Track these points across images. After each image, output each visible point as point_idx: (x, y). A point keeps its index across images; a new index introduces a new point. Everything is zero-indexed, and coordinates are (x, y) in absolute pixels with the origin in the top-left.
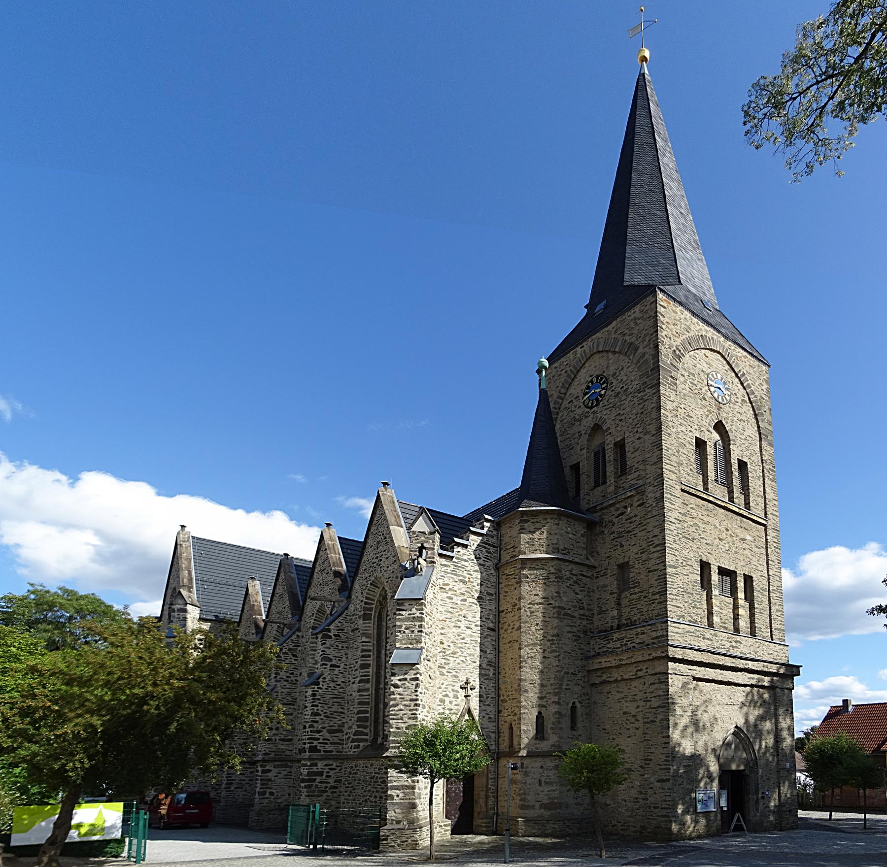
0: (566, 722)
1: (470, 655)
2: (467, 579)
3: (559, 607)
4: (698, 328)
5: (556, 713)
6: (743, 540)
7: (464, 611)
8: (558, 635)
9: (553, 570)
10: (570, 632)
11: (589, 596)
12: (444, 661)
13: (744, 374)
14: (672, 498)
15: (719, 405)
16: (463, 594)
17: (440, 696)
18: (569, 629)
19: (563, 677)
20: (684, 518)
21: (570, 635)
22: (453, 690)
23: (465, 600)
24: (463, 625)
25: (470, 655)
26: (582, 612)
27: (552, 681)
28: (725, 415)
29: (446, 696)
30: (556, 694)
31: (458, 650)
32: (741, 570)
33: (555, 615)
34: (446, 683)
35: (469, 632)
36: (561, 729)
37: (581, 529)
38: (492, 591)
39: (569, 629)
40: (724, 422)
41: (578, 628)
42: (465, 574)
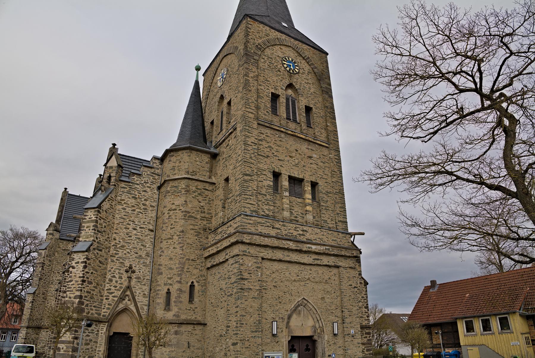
0: (185, 297)
1: (134, 248)
2: (137, 197)
3: (185, 211)
4: (275, 34)
5: (177, 290)
6: (310, 157)
7: (133, 218)
8: (183, 232)
9: (184, 186)
10: (193, 229)
11: (210, 204)
12: (115, 252)
13: (308, 58)
14: (250, 129)
15: (291, 74)
16: (133, 206)
17: (109, 277)
18: (191, 227)
19: (185, 263)
20: (260, 143)
21: (192, 231)
22: (119, 273)
23: (134, 210)
24: (131, 227)
25: (134, 248)
26: (203, 215)
27: (177, 266)
28: (295, 80)
29: (114, 277)
30: (179, 275)
31: (126, 244)
32: (308, 177)
33: (183, 217)
34: (115, 267)
35: (135, 232)
36: (181, 302)
37: (206, 158)
38: (154, 204)
39: (191, 227)
40: (294, 84)
41: (200, 227)
42: (136, 193)
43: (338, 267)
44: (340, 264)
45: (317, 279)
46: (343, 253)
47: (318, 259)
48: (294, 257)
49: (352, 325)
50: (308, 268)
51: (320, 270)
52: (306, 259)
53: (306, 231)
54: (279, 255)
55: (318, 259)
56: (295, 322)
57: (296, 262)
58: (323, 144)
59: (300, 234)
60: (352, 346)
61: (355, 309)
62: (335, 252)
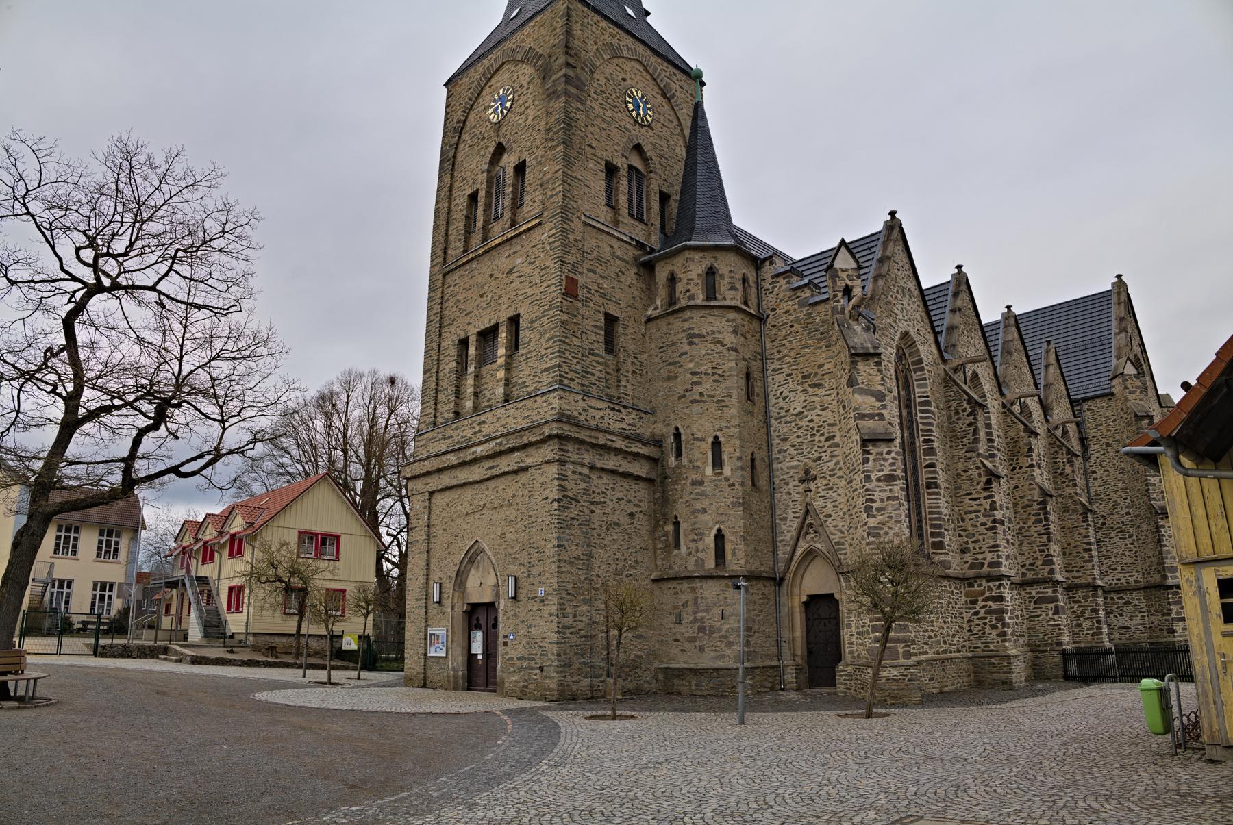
43: (526, 469)
44: (529, 461)
45: (496, 504)
46: (525, 440)
47: (492, 467)
48: (463, 476)
49: (543, 579)
50: (483, 486)
51: (500, 484)
52: (476, 473)
53: (484, 422)
54: (446, 480)
55: (492, 467)
56: (473, 580)
57: (465, 485)
58: (530, 225)
59: (475, 433)
60: (538, 621)
61: (551, 545)
62: (513, 443)
